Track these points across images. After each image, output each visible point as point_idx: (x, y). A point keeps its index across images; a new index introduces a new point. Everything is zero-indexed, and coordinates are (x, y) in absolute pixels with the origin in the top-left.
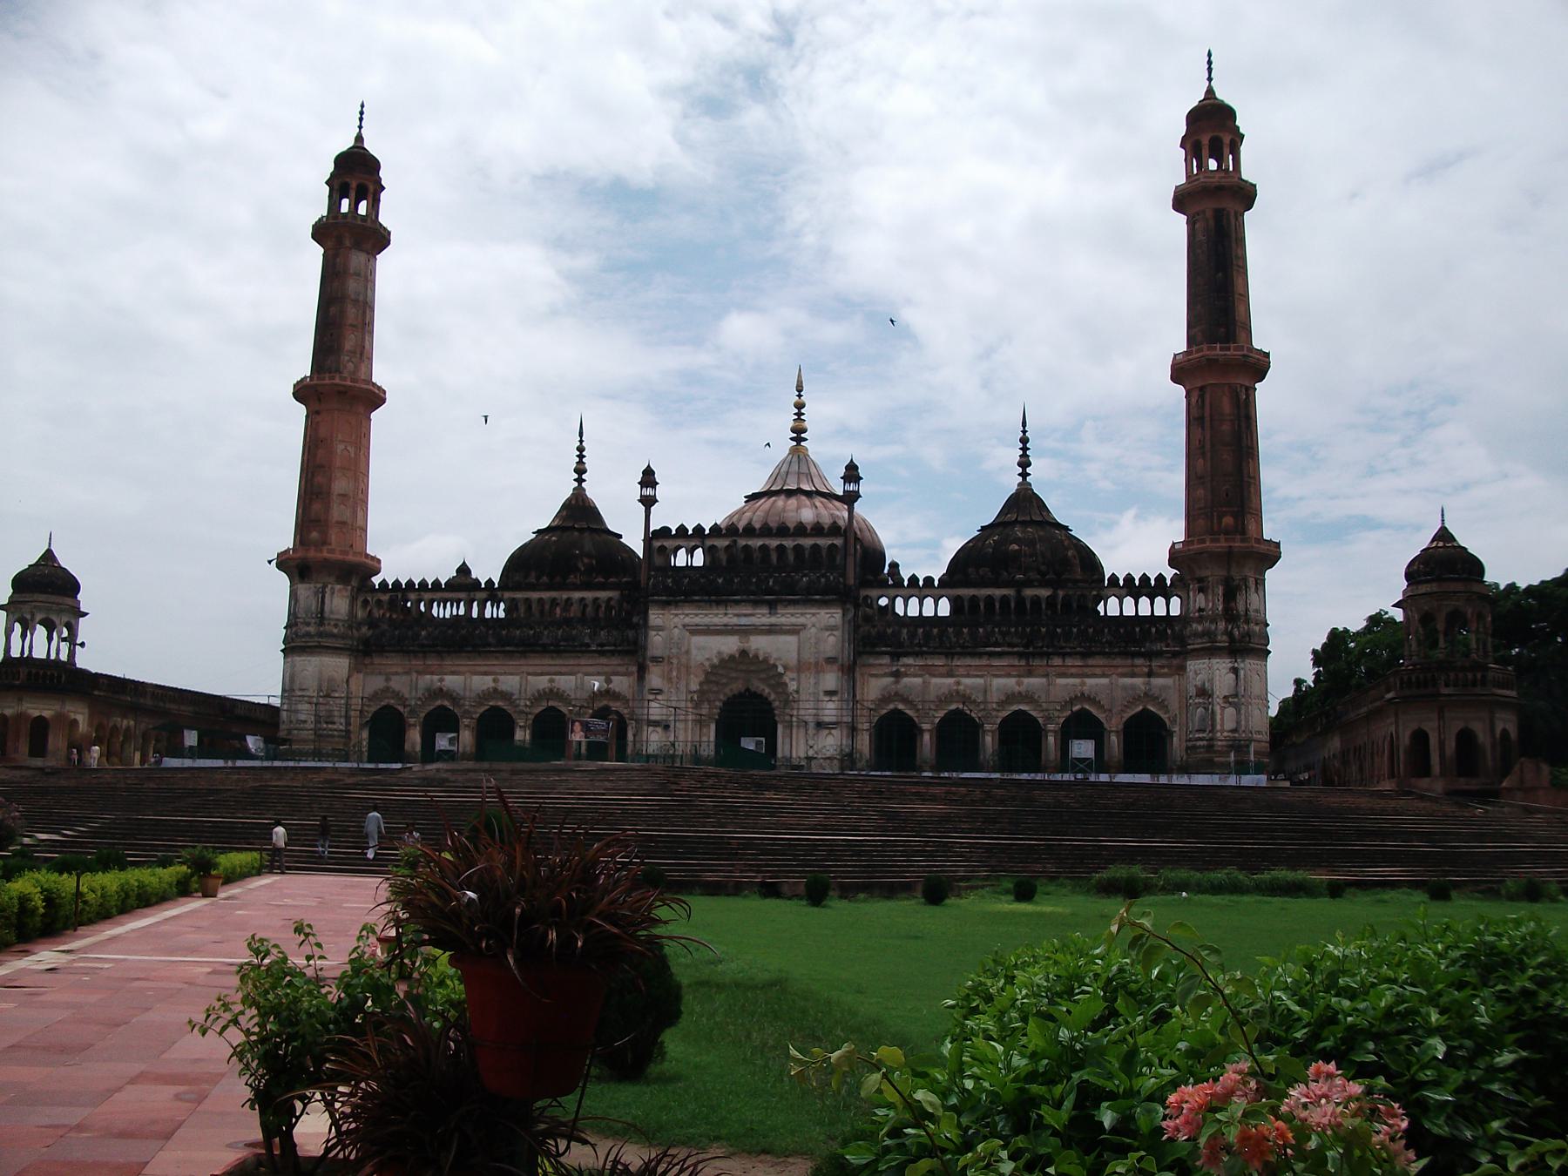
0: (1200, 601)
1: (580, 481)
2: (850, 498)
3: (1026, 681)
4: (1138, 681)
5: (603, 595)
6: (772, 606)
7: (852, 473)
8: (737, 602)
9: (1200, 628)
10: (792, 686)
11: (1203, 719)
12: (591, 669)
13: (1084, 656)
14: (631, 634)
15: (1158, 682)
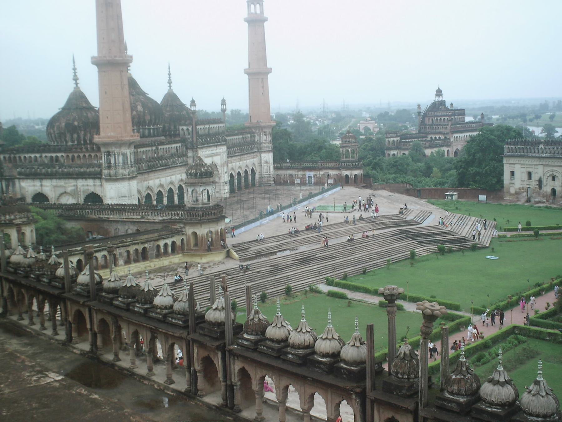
0: (265, 137)
1: (77, 84)
2: (224, 111)
3: (241, 162)
4: (252, 160)
5: (179, 145)
6: (216, 146)
7: (223, 102)
8: (212, 146)
9: (265, 145)
10: (220, 172)
11: (267, 169)
12: (177, 172)
13: (247, 154)
14: (184, 158)
15: (255, 159)
